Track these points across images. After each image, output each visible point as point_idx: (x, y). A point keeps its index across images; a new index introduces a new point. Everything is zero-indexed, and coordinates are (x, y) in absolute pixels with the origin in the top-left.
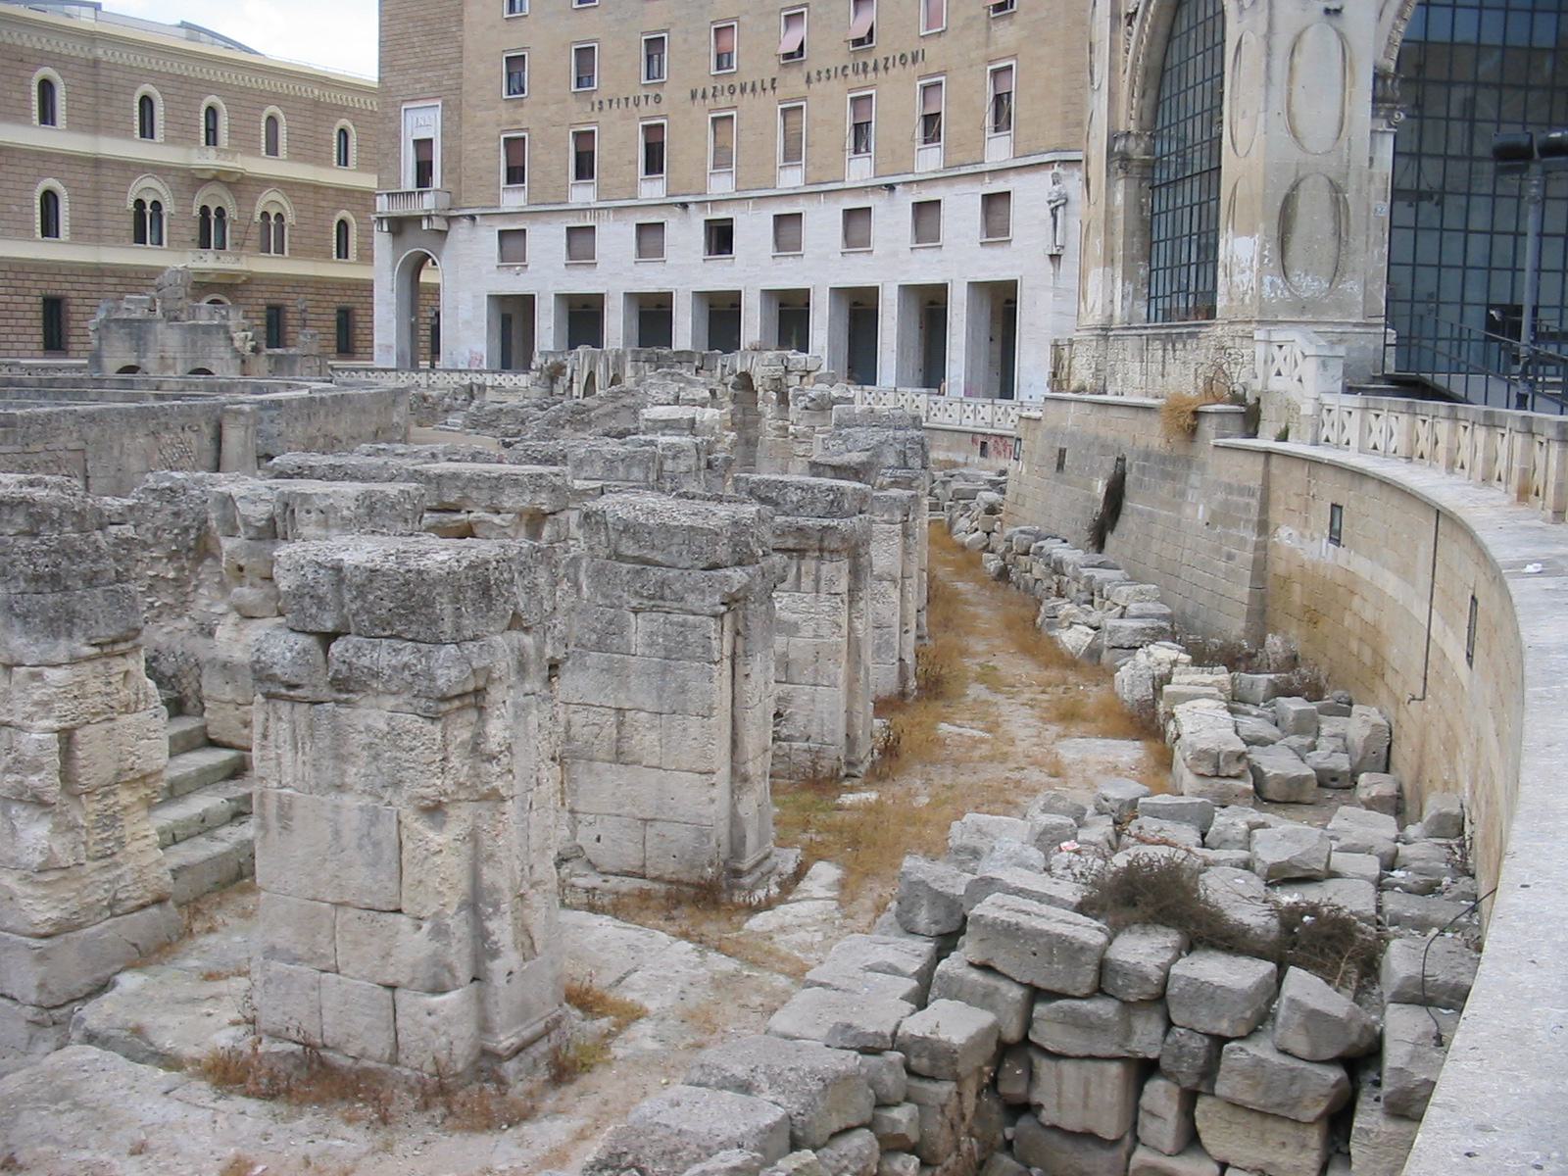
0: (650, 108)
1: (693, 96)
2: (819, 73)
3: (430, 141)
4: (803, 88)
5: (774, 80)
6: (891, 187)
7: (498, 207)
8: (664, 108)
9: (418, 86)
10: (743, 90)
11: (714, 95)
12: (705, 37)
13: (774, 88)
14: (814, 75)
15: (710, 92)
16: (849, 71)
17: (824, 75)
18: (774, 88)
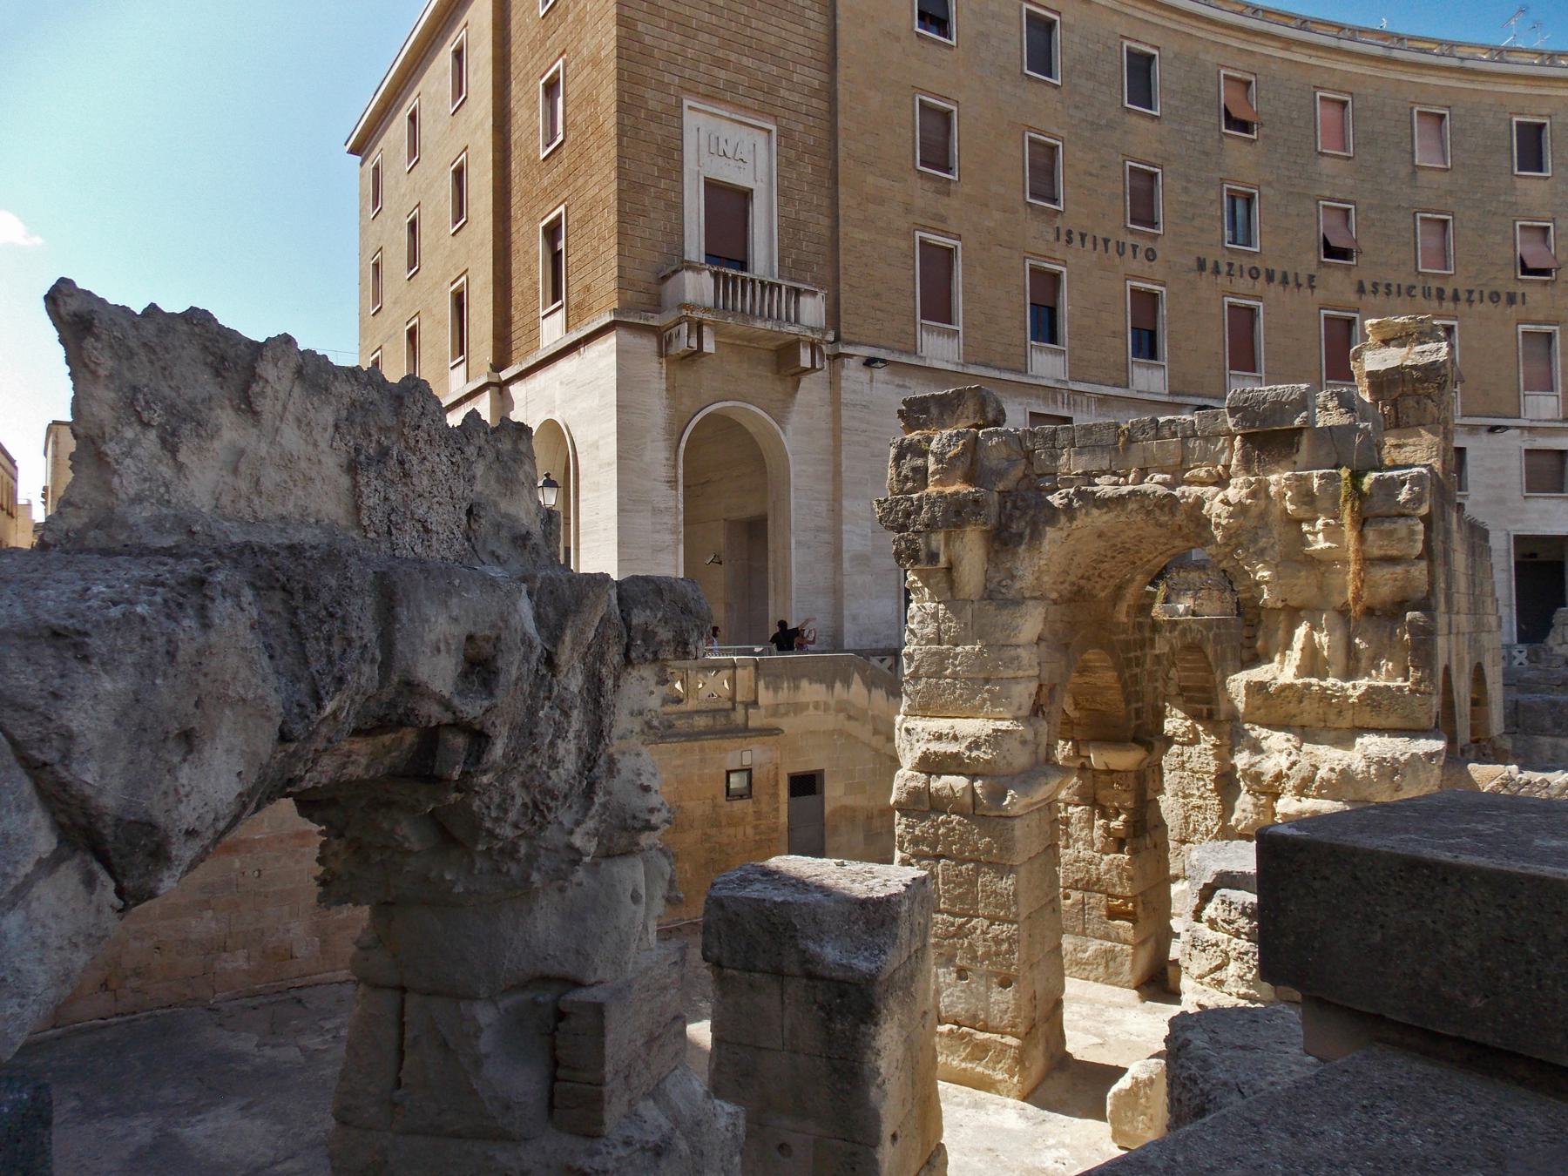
0: (1138, 265)
1: (1201, 265)
2: (1375, 285)
3: (746, 195)
4: (1352, 297)
5: (1311, 278)
6: (1492, 429)
7: (913, 352)
8: (1158, 269)
9: (722, 74)
10: (1270, 277)
11: (1229, 274)
12: (1213, 195)
13: (1312, 287)
14: (1368, 286)
15: (1224, 269)
16: (1418, 292)
17: (1382, 289)
18: (1312, 287)
